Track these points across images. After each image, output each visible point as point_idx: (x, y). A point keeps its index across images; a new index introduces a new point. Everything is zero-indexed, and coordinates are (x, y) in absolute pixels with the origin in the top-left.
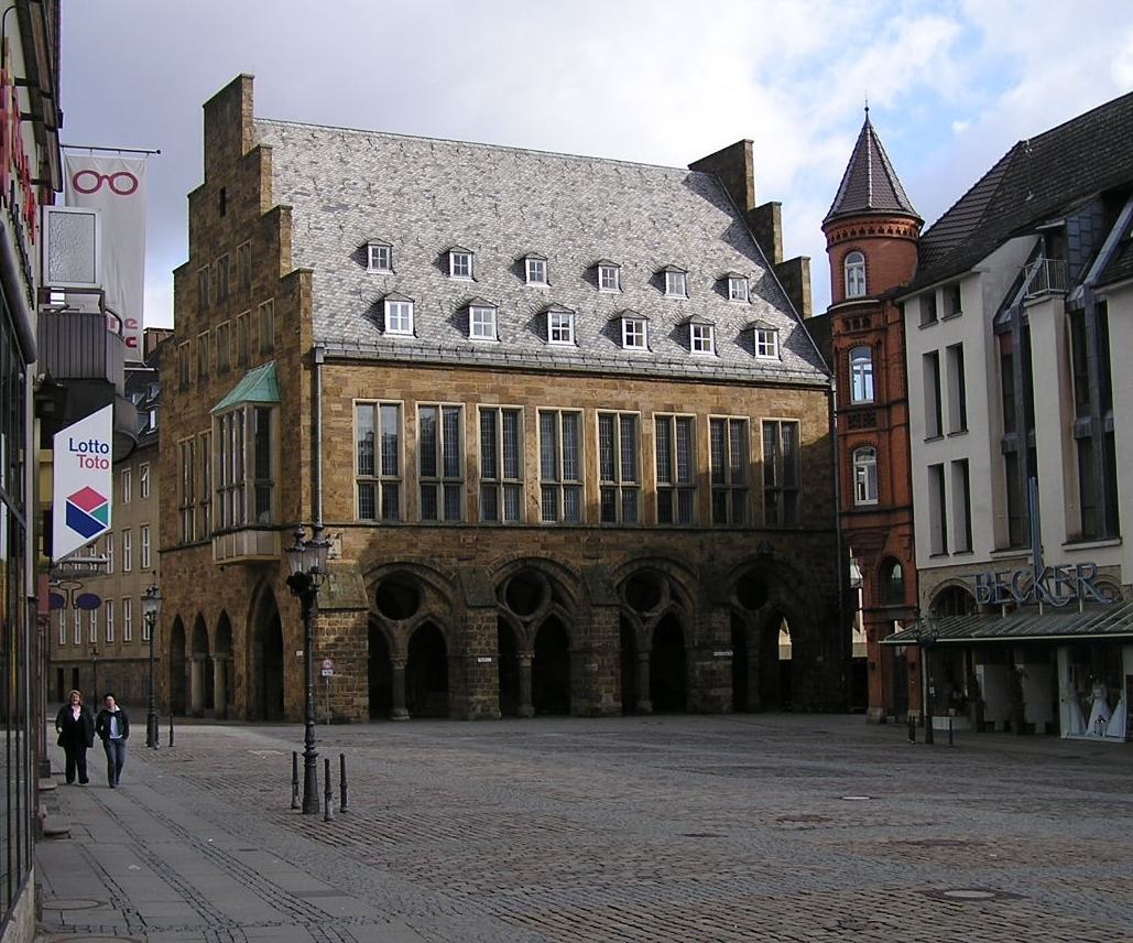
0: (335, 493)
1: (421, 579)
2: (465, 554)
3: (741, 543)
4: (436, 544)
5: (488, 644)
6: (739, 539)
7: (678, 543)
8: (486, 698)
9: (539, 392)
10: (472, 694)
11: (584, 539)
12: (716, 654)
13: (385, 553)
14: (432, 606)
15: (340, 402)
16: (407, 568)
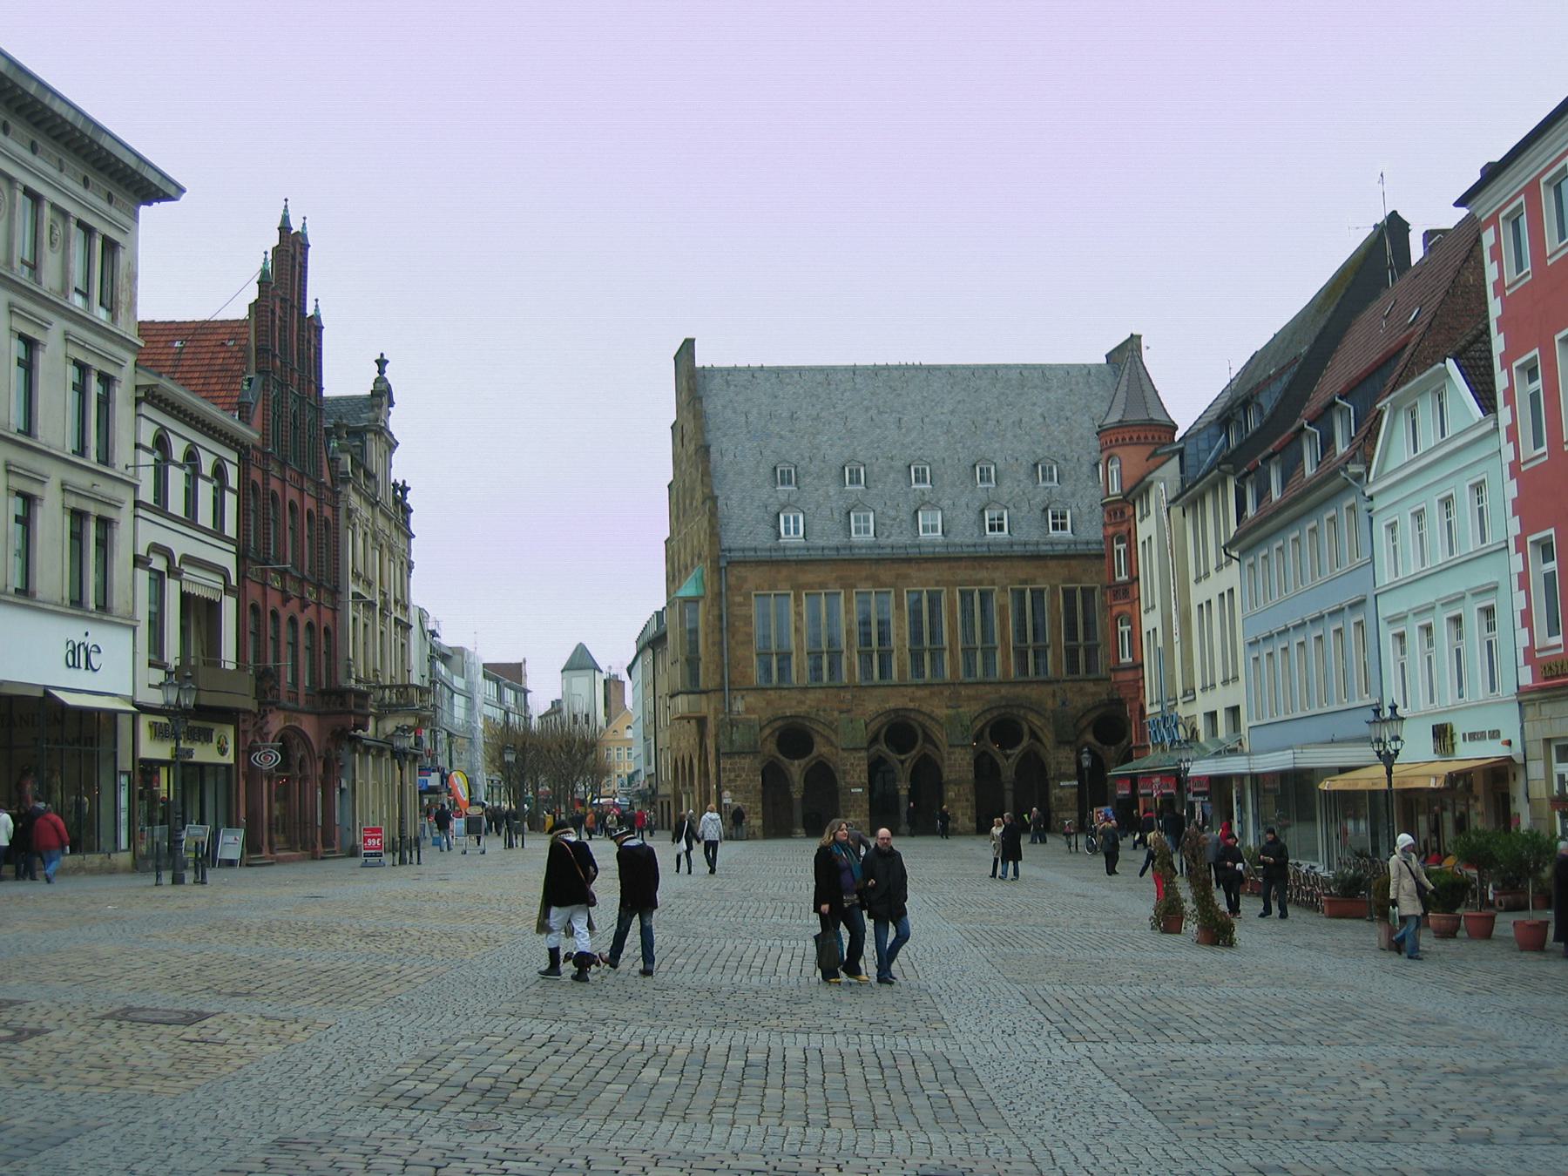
2: (844, 707)
6: (1090, 688)
7: (1032, 692)
11: (947, 693)
14: (821, 749)
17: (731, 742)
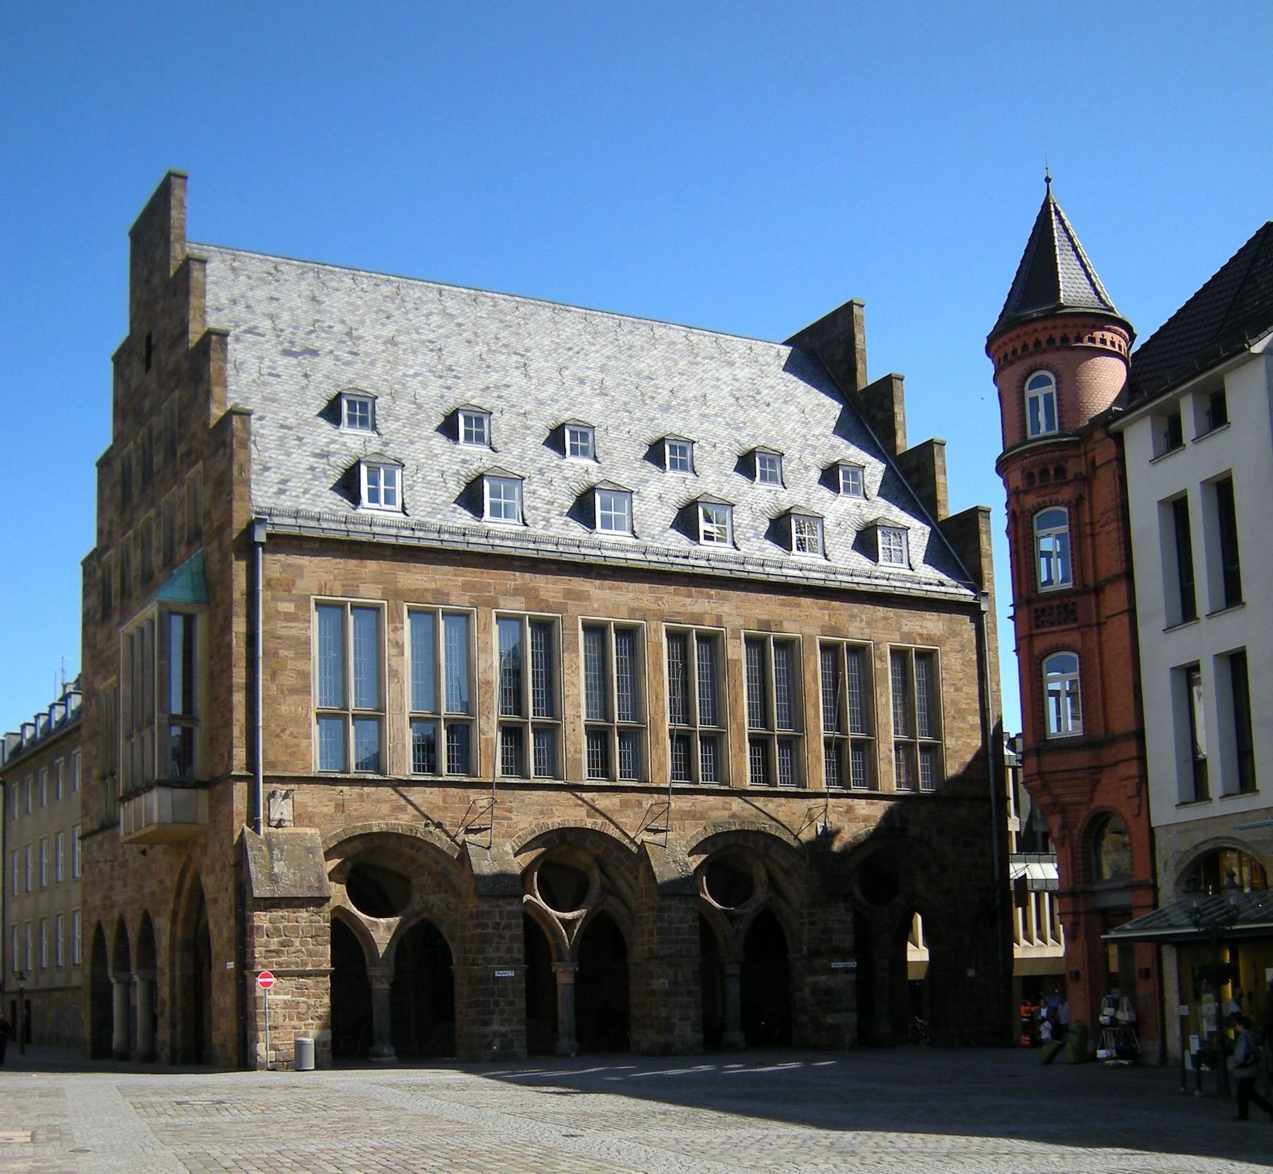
0: (283, 731)
3: (863, 812)
5: (509, 950)
8: (507, 1029)
9: (581, 596)
10: (486, 1023)
12: (833, 965)
15: (290, 601)
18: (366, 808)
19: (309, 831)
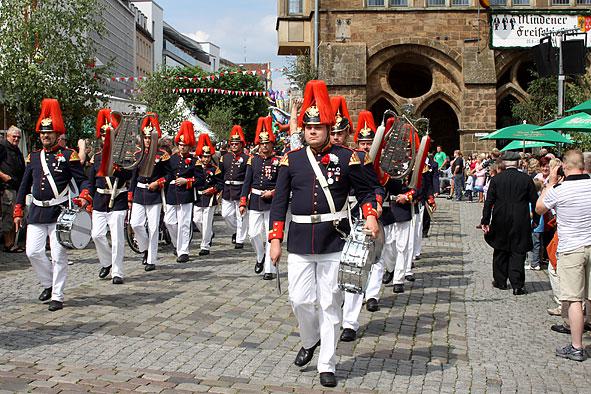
1: (431, 61)
2: (470, 35)
4: (441, 27)
5: (485, 120)
13: (391, 36)
14: (439, 84)
16: (416, 50)
17: (332, 74)
18: (397, 29)
19: (359, 44)
